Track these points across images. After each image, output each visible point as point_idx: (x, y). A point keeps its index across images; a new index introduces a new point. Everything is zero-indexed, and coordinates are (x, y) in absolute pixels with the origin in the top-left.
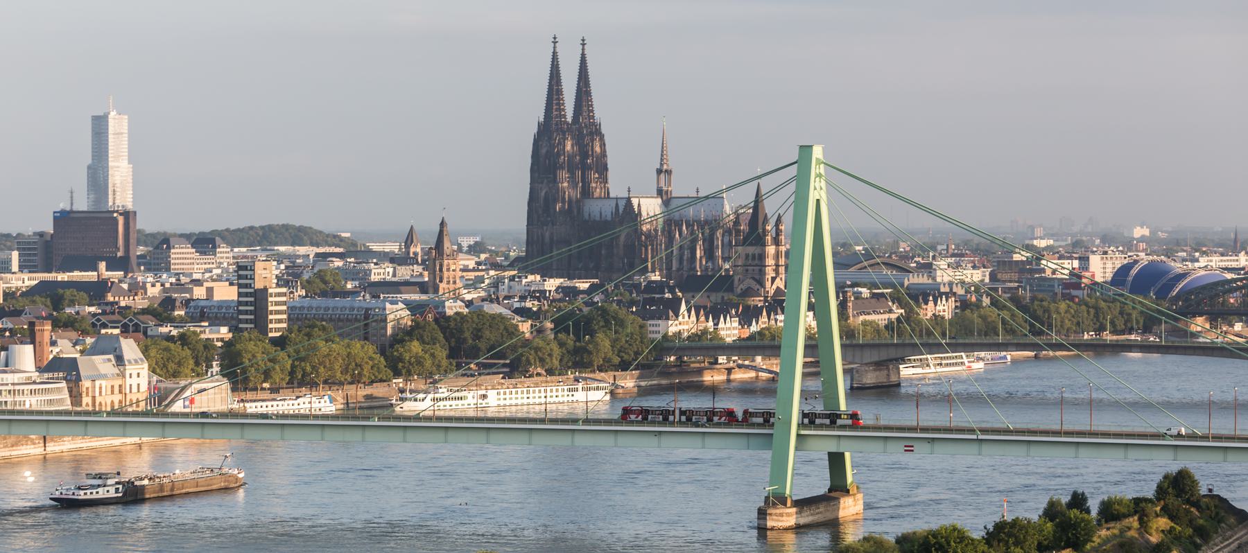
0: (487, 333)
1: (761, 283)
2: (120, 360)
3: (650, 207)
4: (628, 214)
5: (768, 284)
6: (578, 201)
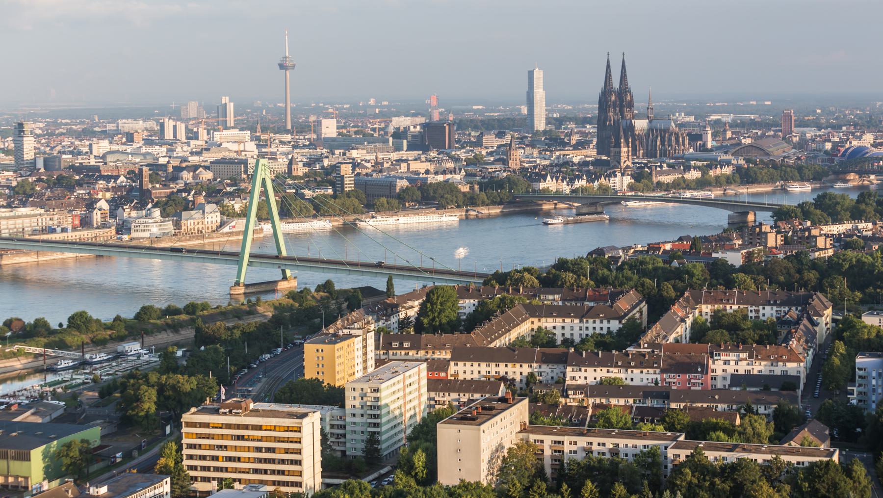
0: (440, 191)
1: (619, 163)
3: (641, 125)
5: (622, 164)
6: (618, 120)
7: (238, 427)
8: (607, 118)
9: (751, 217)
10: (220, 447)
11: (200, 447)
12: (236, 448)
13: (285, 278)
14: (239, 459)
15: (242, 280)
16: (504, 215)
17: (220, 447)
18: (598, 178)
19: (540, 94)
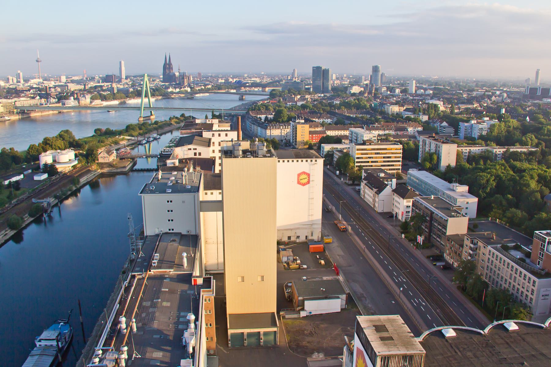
2: (85, 98)
3: (177, 74)
4: (175, 75)
7: (378, 149)
8: (166, 72)
9: (244, 97)
10: (369, 158)
11: (362, 158)
12: (376, 158)
13: (152, 115)
14: (377, 162)
15: (142, 116)
16: (162, 99)
17: (369, 158)
18: (182, 88)
19: (123, 68)
